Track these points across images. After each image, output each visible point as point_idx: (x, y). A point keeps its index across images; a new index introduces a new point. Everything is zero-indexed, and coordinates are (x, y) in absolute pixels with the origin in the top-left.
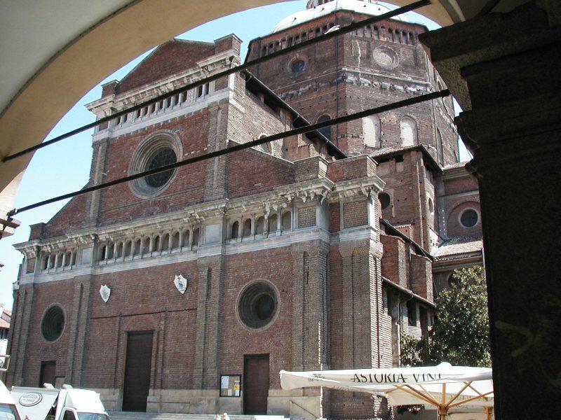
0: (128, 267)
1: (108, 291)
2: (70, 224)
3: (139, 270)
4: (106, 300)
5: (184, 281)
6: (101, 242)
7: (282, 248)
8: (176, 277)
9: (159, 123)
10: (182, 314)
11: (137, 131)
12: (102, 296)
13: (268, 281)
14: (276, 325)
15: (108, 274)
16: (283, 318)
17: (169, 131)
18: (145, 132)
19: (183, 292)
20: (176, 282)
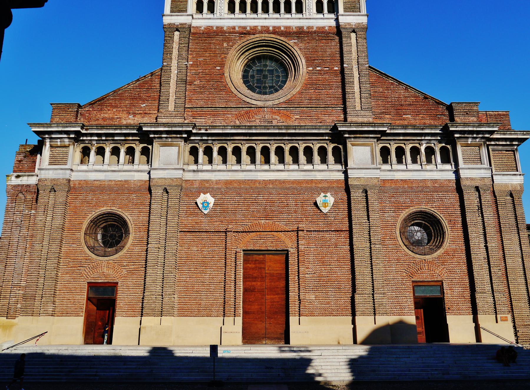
0: (241, 176)
1: (211, 200)
2: (129, 114)
3: (259, 182)
4: (206, 212)
5: (331, 200)
6: (193, 141)
7: (446, 180)
8: (322, 194)
9: (268, 27)
10: (327, 235)
11: (234, 28)
12: (200, 206)
13: (432, 209)
14: (446, 253)
15: (207, 181)
16: (454, 247)
17: (282, 38)
18: (244, 32)
19: (325, 210)
20: (320, 200)
